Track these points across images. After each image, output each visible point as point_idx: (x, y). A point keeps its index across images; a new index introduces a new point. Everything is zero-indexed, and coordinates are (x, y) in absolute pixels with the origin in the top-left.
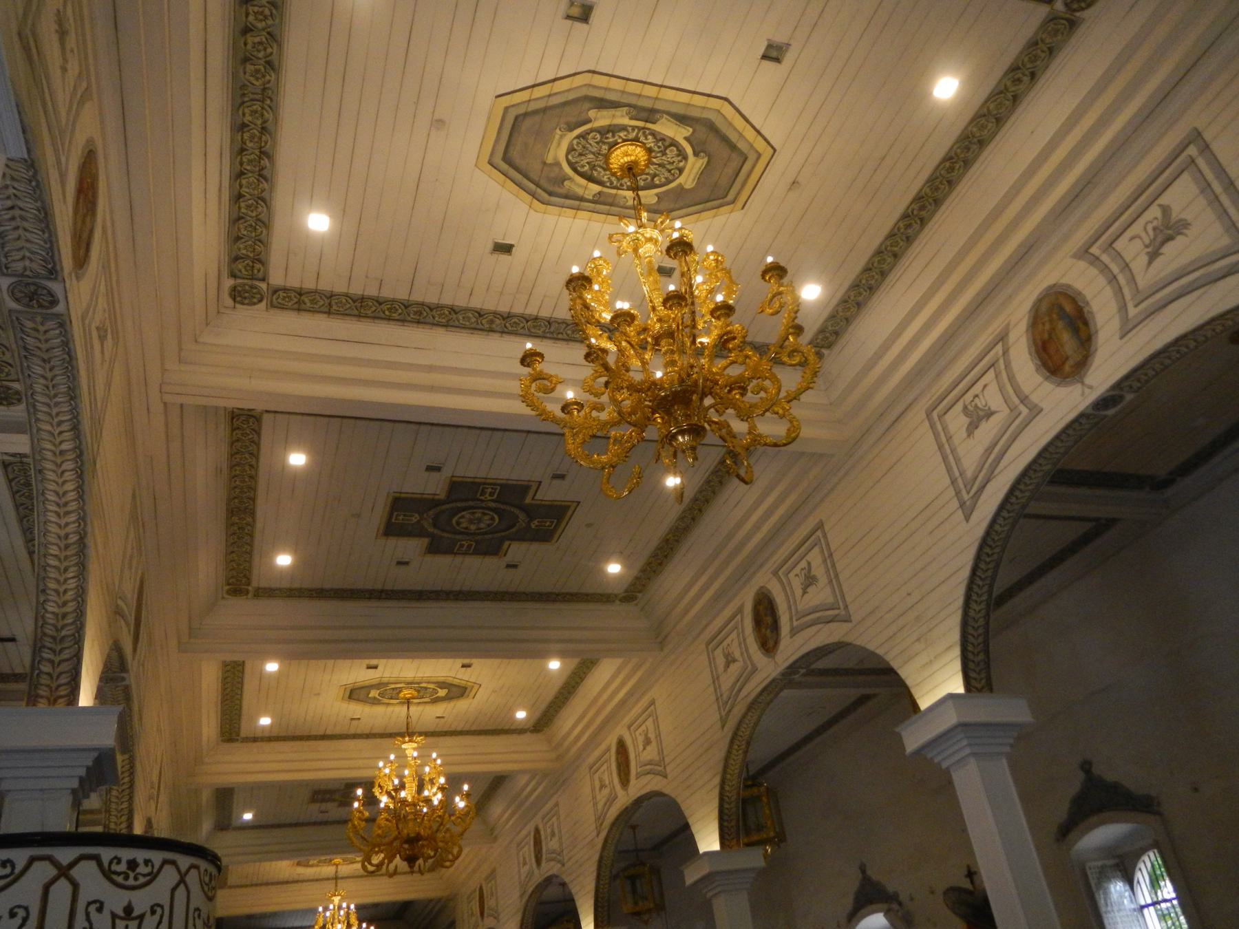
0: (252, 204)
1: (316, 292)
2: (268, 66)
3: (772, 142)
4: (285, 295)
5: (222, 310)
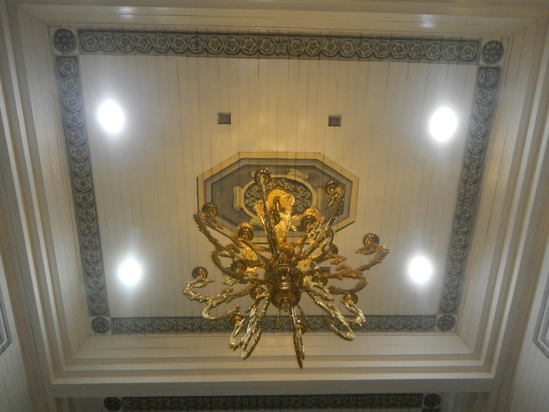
2: (459, 217)
4: (469, 56)
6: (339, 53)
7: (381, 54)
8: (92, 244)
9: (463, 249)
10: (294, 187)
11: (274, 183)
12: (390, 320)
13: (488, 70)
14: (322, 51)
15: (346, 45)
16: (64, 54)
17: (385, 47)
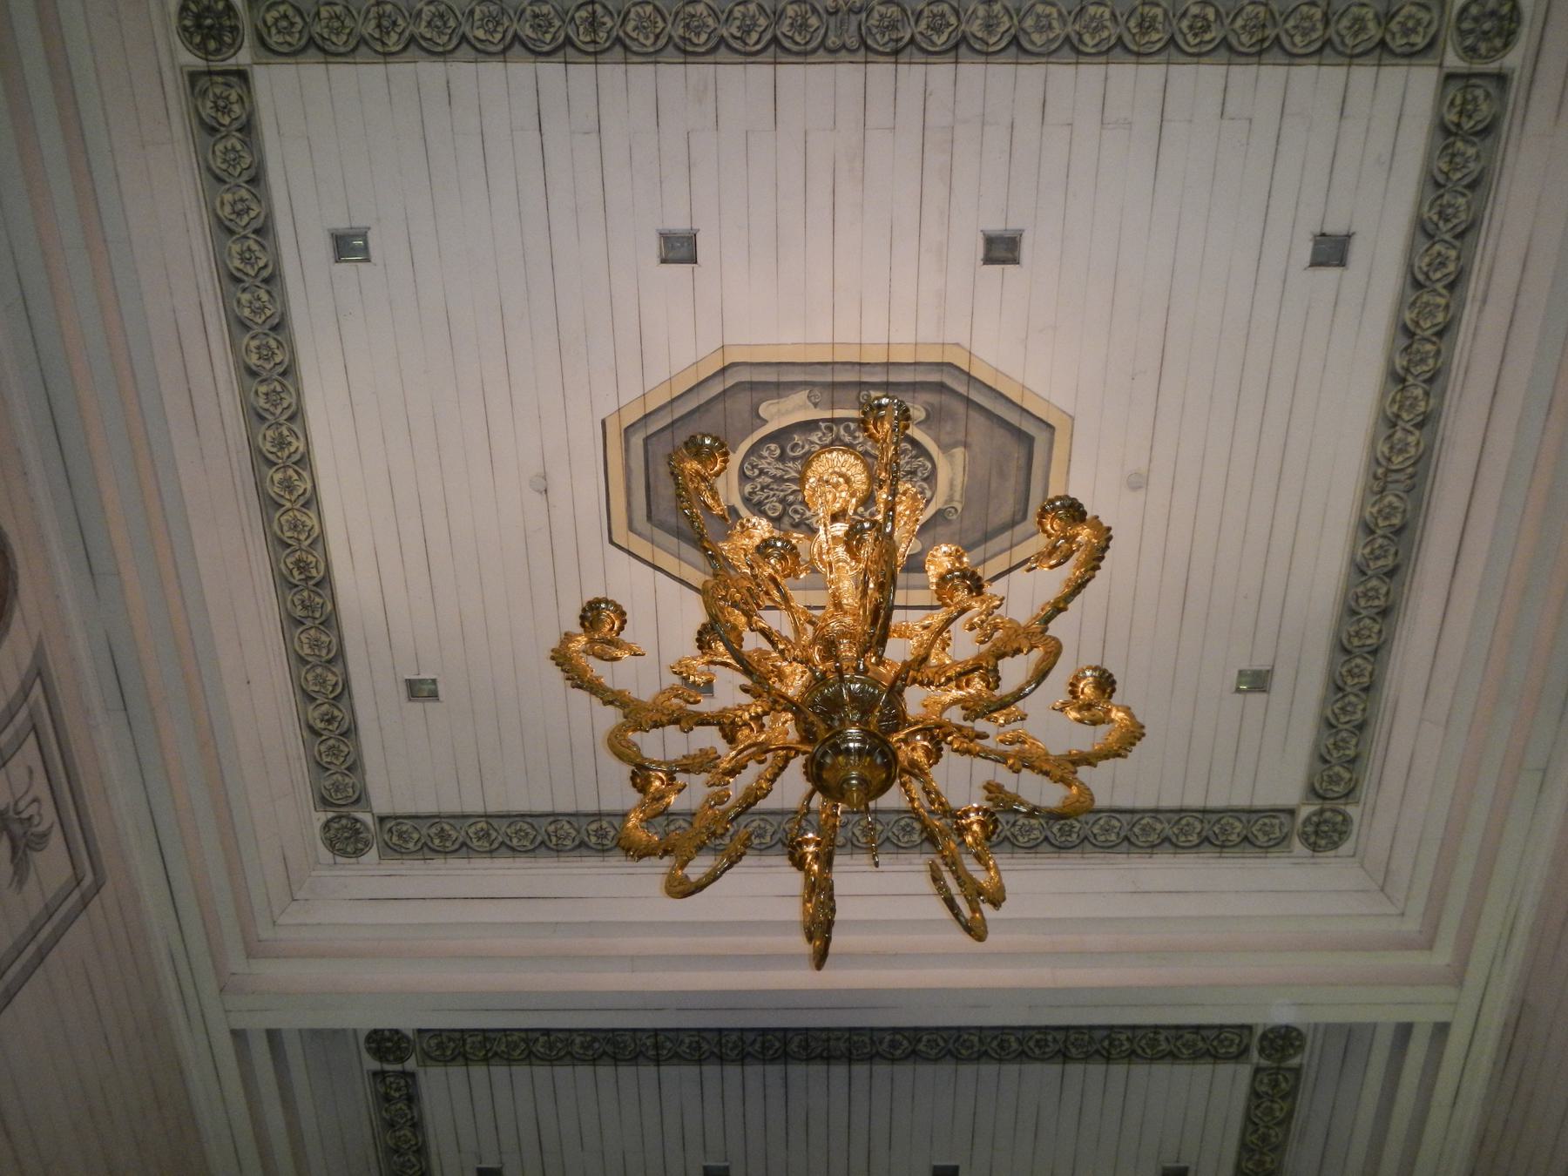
0: (1436, 270)
2: (1372, 526)
3: (625, 555)
6: (1015, 41)
7: (1143, 42)
8: (313, 612)
9: (1380, 620)
11: (824, 434)
12: (1161, 822)
13: (1473, 81)
14: (964, 39)
15: (1038, 16)
16: (211, 63)
17: (1154, 18)
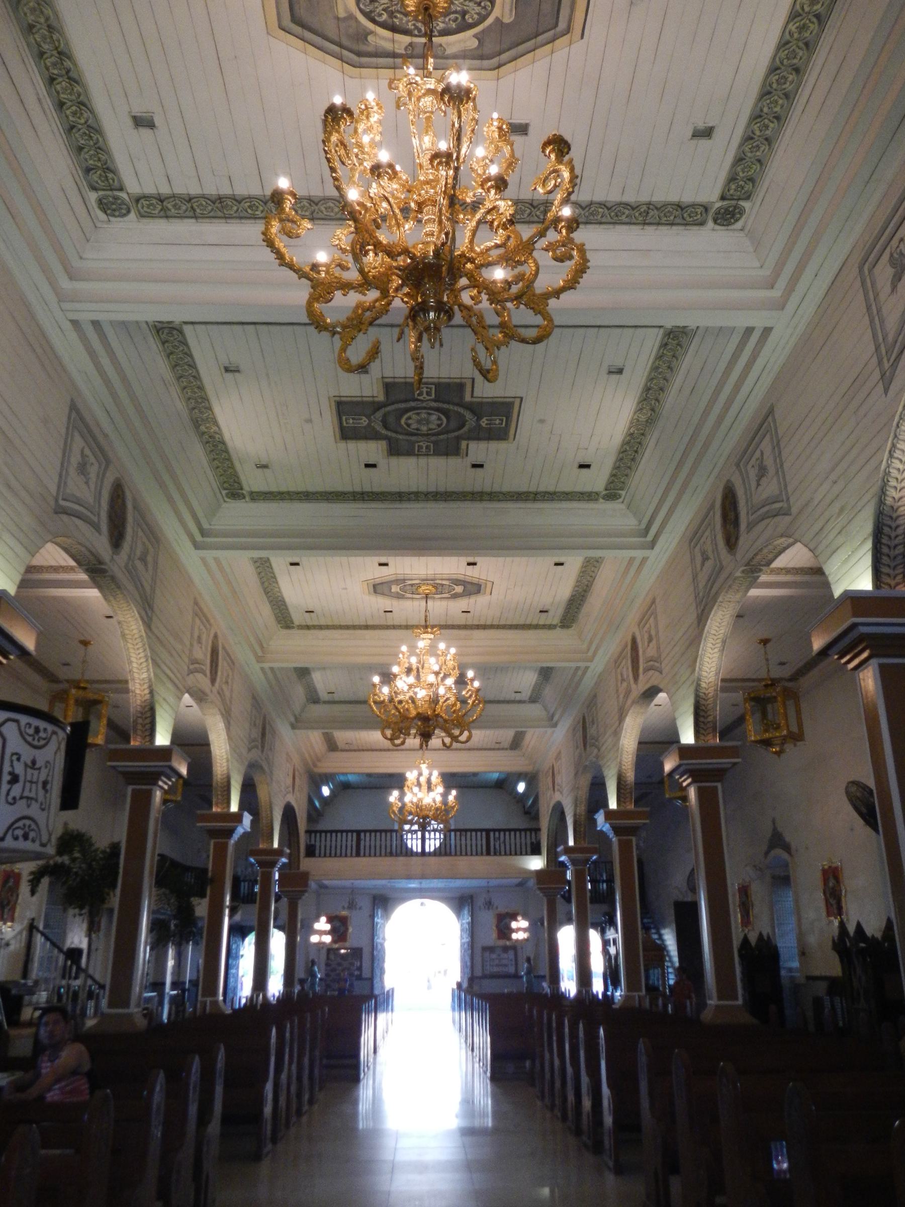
1: (174, 196)
5: (99, 225)
10: (395, 20)
